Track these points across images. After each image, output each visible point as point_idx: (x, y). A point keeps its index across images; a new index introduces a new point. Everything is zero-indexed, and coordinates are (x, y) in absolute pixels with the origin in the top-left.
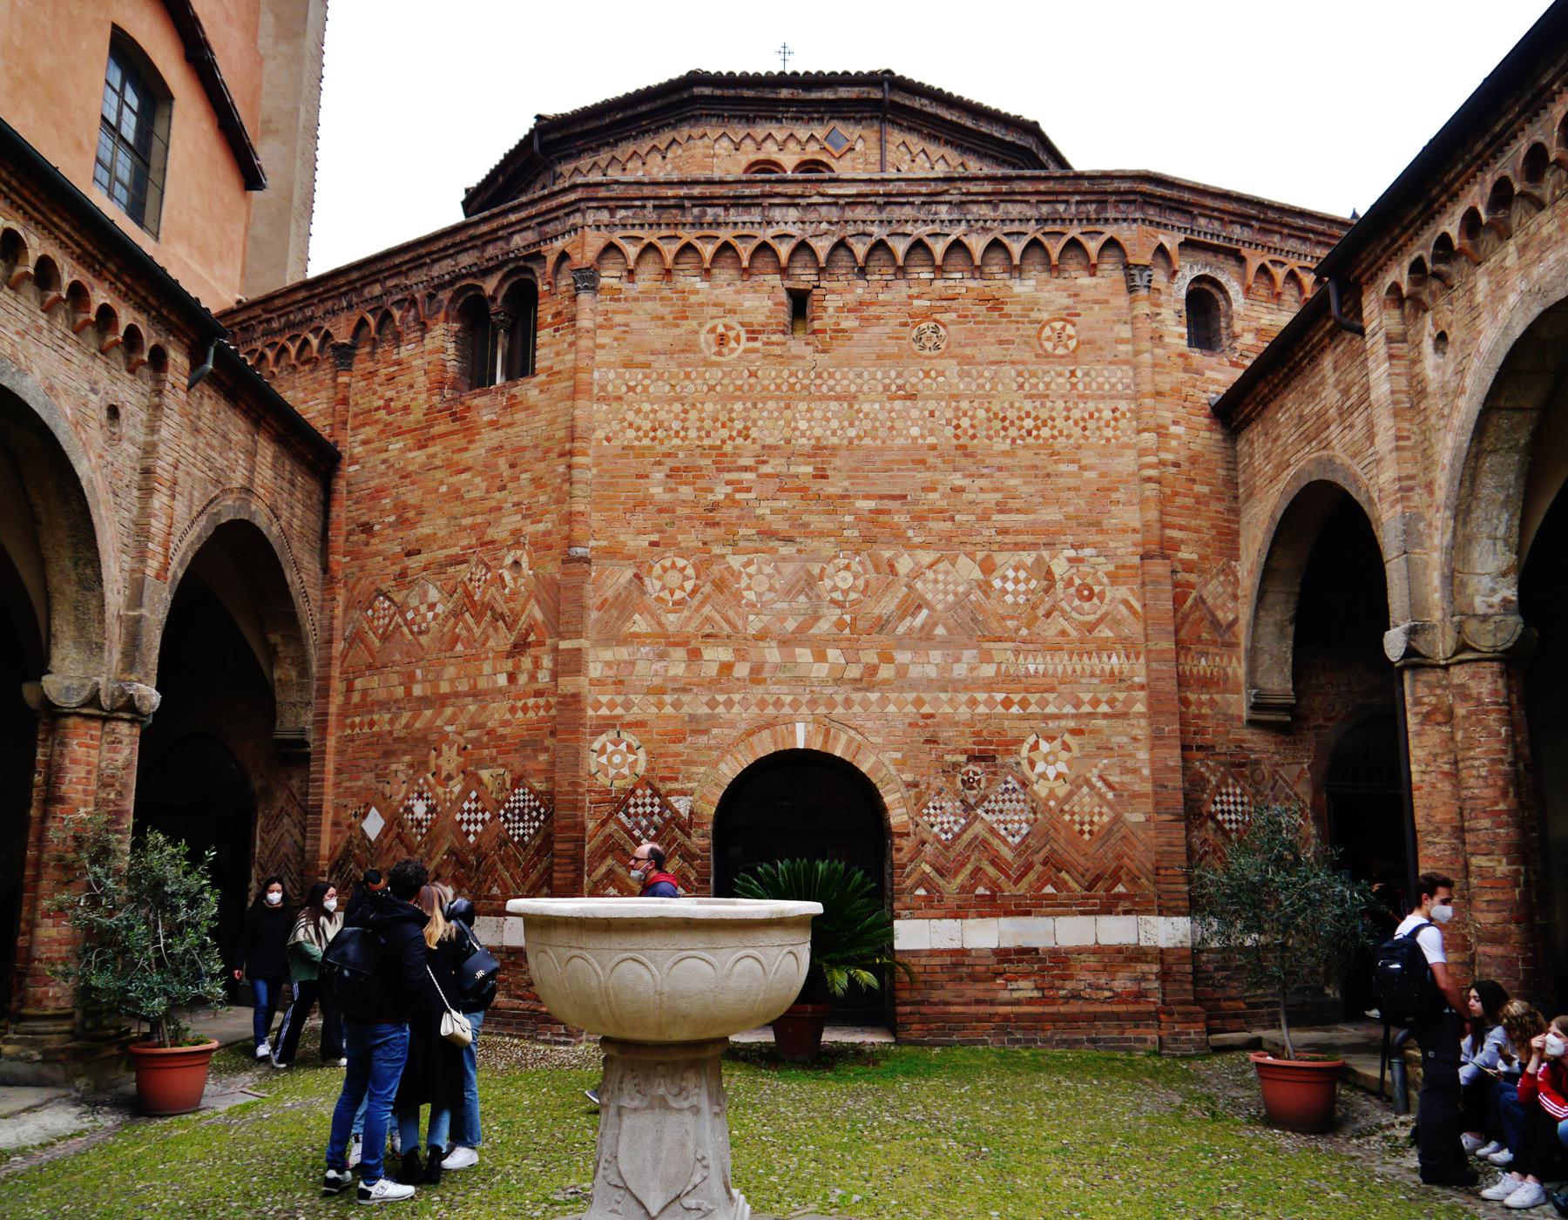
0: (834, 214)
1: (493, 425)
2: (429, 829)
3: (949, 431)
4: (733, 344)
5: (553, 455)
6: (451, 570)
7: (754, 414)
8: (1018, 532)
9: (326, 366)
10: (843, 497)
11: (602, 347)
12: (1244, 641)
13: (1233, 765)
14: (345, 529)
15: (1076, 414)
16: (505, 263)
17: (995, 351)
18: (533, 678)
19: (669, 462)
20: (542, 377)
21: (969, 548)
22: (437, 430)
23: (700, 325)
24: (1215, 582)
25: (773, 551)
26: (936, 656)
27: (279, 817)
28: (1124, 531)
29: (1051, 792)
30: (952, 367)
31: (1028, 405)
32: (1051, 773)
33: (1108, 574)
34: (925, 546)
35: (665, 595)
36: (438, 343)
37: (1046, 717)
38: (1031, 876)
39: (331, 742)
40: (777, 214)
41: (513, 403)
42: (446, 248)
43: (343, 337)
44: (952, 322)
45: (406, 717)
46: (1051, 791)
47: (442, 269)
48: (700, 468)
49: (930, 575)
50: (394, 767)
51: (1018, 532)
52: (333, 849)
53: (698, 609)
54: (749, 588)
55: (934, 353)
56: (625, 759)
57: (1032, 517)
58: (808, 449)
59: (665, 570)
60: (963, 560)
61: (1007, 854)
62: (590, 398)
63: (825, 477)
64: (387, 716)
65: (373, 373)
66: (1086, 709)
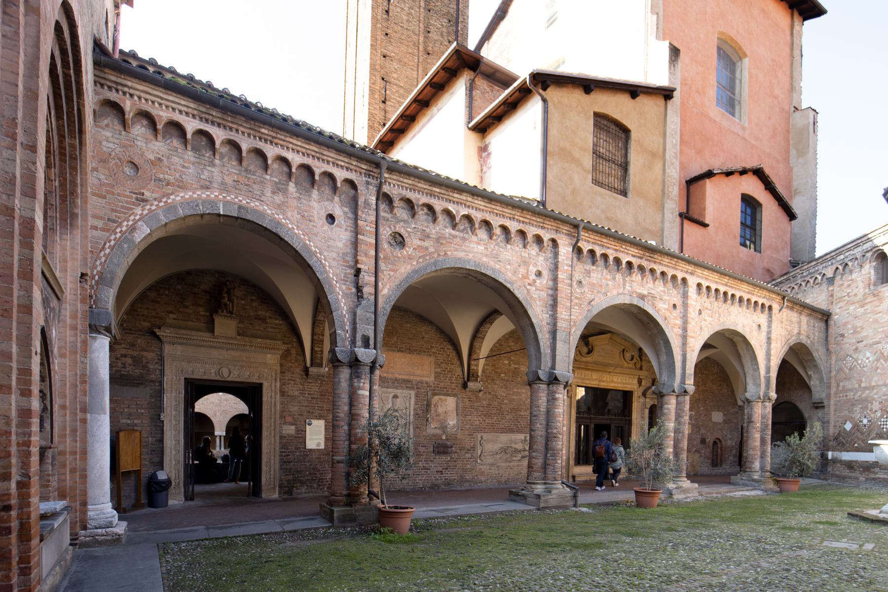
2: (869, 427)
6: (875, 346)
9: (824, 285)
14: (834, 336)
39: (832, 402)
45: (859, 393)
64: (852, 394)
65: (842, 285)
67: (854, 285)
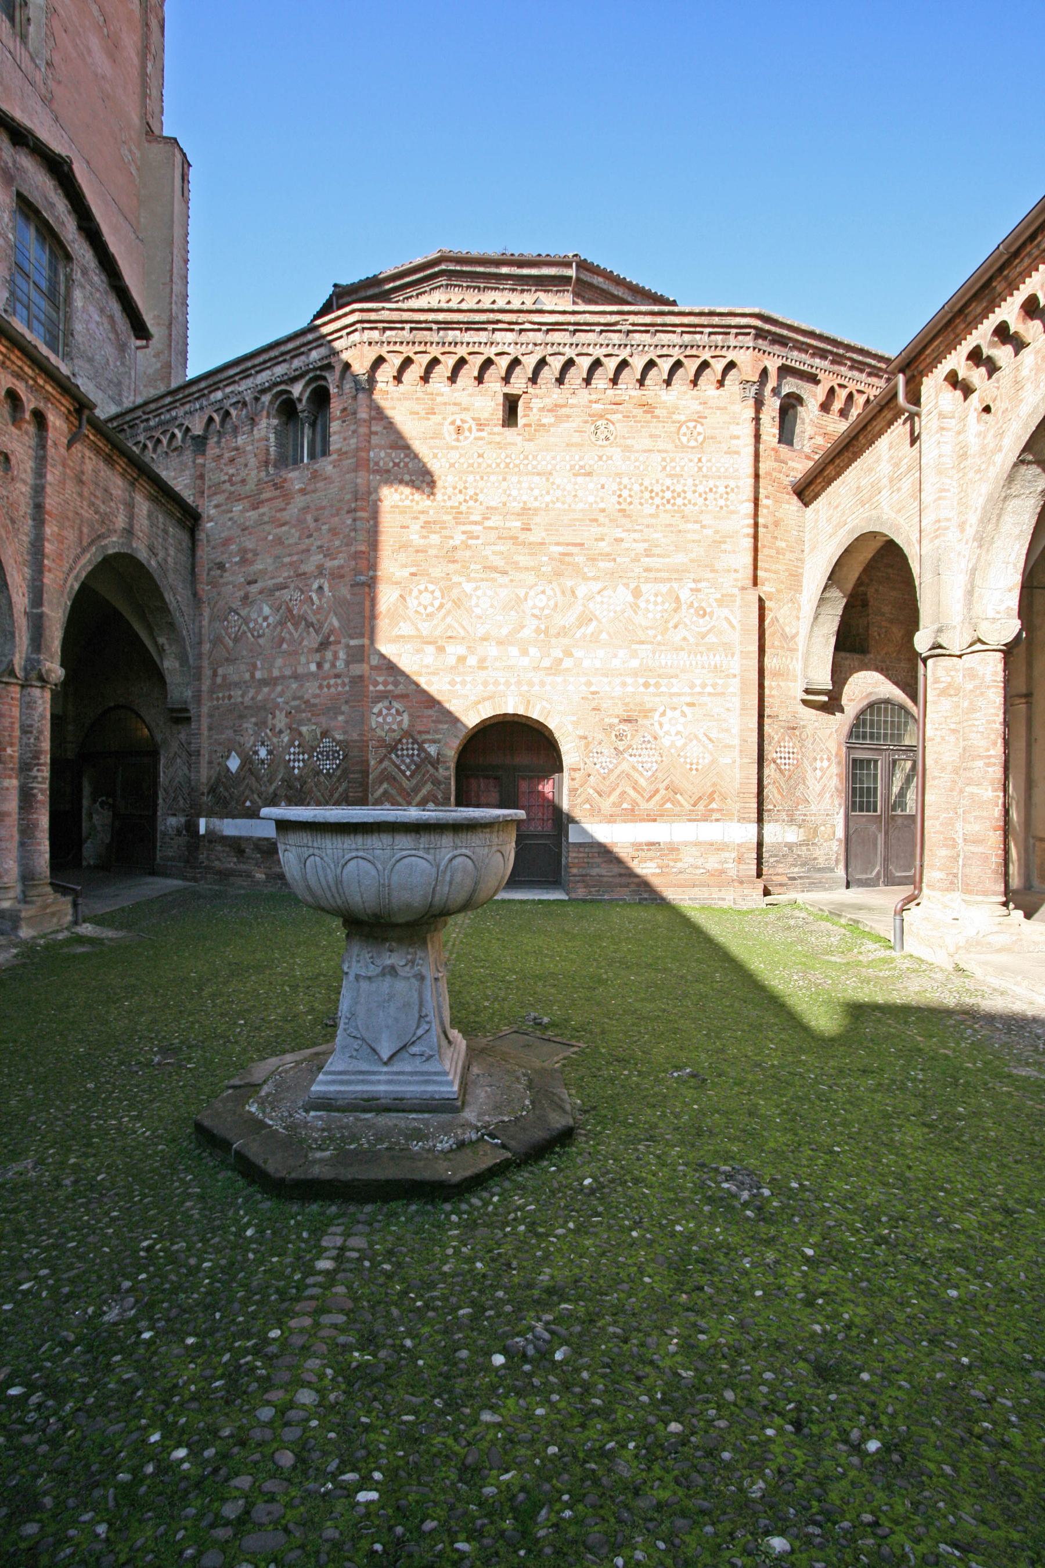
0: (539, 337)
1: (303, 491)
3: (615, 499)
4: (467, 433)
5: (344, 512)
6: (277, 594)
7: (481, 484)
8: (659, 570)
10: (542, 544)
11: (376, 433)
12: (801, 647)
13: (789, 728)
15: (701, 489)
16: (307, 372)
17: (648, 443)
18: (333, 665)
19: (423, 518)
20: (334, 457)
21: (625, 581)
22: (265, 496)
23: (444, 419)
24: (786, 608)
25: (494, 580)
26: (601, 653)
27: (174, 758)
28: (729, 571)
29: (673, 745)
30: (616, 452)
31: (668, 482)
32: (673, 731)
33: (716, 600)
34: (596, 579)
35: (421, 609)
36: (263, 433)
37: (672, 695)
38: (657, 797)
39: (205, 710)
40: (498, 336)
41: (315, 476)
42: (265, 362)
43: (198, 430)
44: (619, 421)
45: (252, 693)
46: (673, 742)
47: (263, 378)
48: (444, 522)
49: (598, 598)
50: (245, 725)
51: (659, 570)
52: (209, 778)
53: (444, 618)
54: (477, 606)
55: (605, 443)
56: (394, 719)
57: (667, 560)
58: (518, 509)
59: (420, 592)
60: (621, 588)
61: (642, 782)
62: (368, 471)
63: (529, 530)
65: (220, 457)
66: (698, 689)
67: (240, 460)
